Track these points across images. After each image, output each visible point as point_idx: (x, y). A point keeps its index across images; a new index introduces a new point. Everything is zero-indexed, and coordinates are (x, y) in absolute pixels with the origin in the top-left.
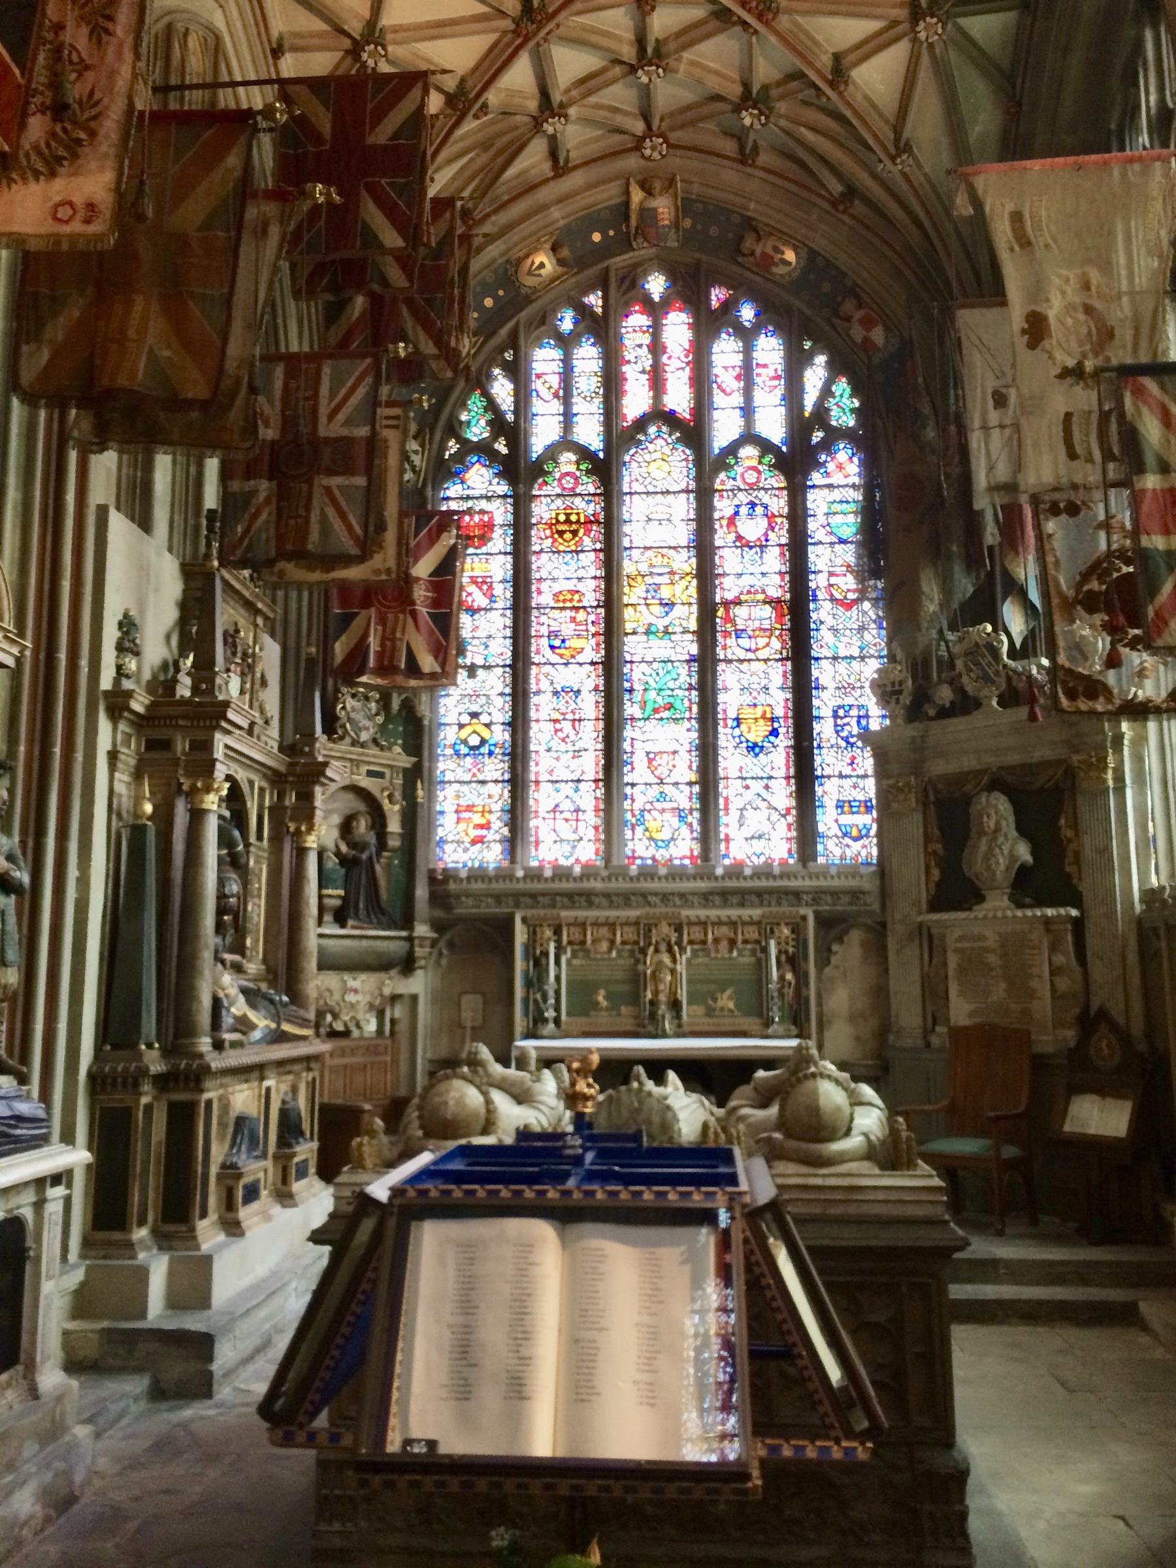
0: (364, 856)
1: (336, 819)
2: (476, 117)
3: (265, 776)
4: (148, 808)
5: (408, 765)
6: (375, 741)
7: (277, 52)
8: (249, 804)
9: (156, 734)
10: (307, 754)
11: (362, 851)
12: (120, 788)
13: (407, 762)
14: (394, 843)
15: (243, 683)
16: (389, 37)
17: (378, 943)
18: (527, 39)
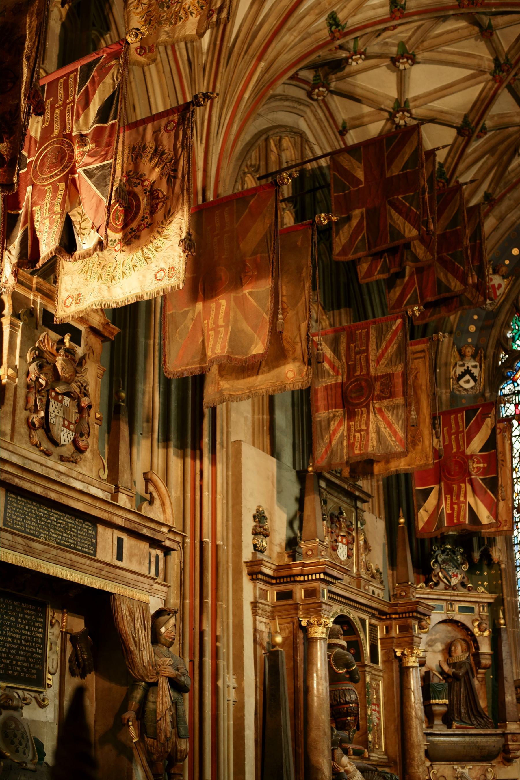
0: (461, 673)
1: (439, 646)
2: (479, 137)
3: (373, 616)
4: (279, 639)
5: (491, 601)
6: (463, 585)
7: (343, 132)
8: (362, 636)
9: (281, 588)
10: (404, 597)
11: (461, 668)
12: (261, 627)
13: (489, 598)
14: (486, 661)
15: (350, 550)
16: (411, 104)
17: (479, 739)
18: (501, 82)
